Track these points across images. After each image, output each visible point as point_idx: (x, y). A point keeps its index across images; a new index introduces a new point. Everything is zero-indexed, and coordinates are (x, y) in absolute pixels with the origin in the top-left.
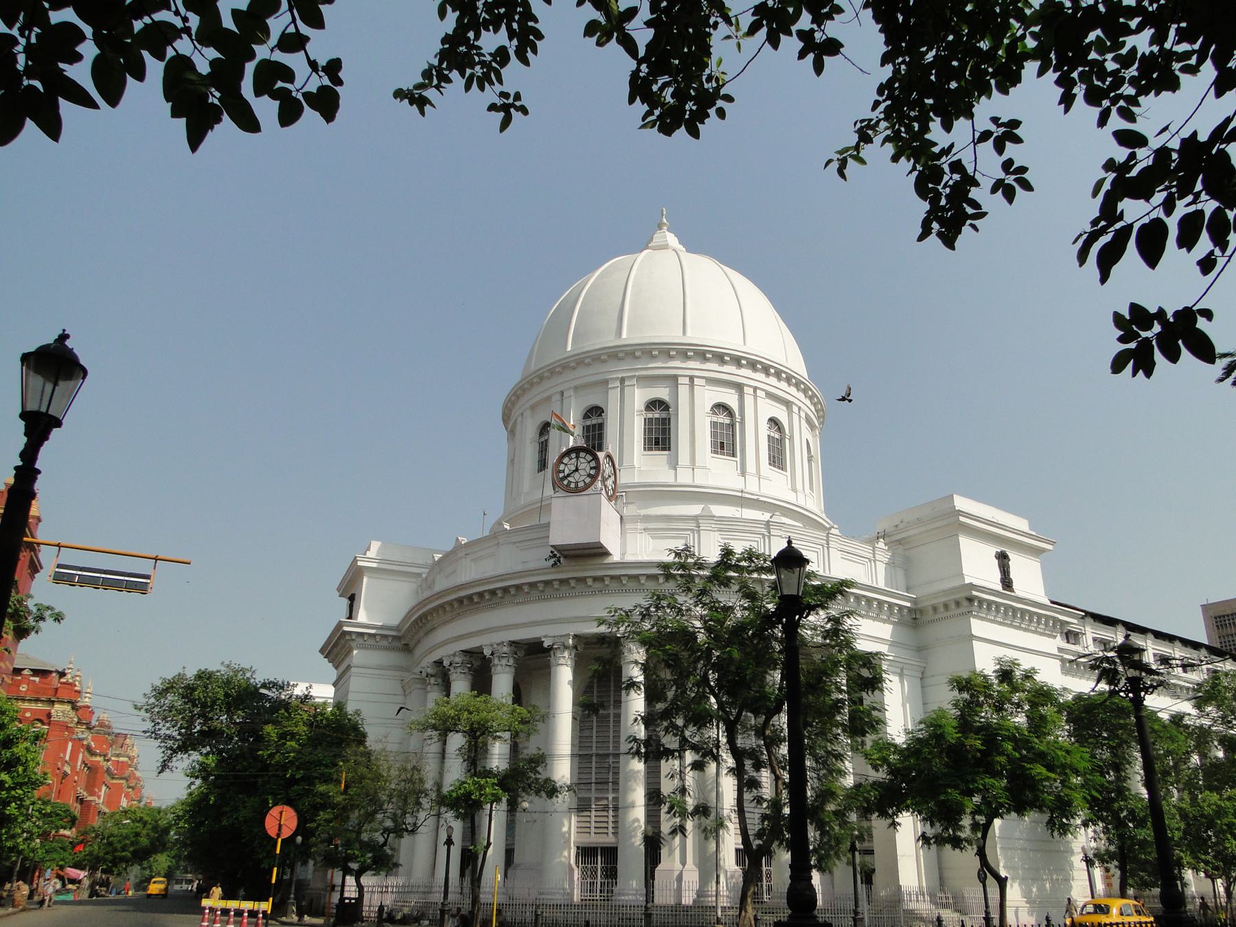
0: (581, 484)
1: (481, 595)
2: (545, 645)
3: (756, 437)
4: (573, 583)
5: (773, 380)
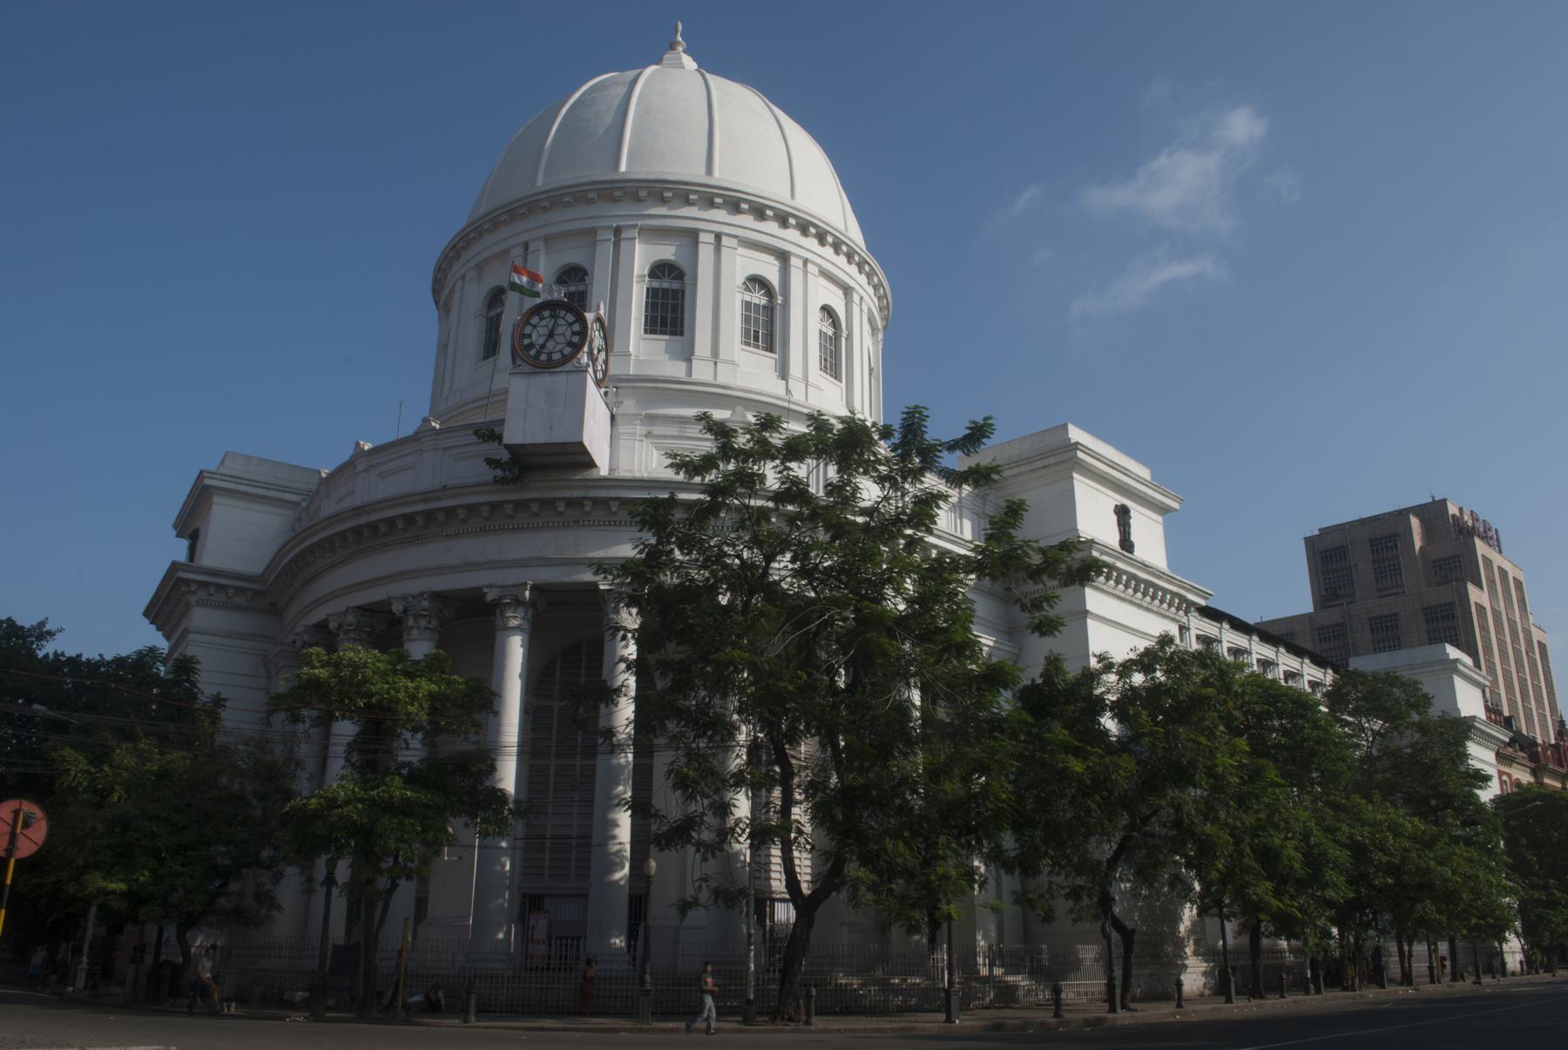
0: (557, 356)
1: (391, 522)
2: (489, 598)
3: (805, 330)
4: (535, 507)
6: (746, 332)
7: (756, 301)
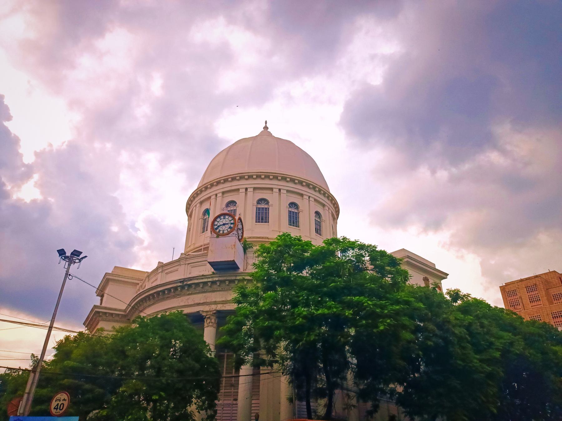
0: (225, 232)
5: (317, 194)
6: (290, 221)
7: (293, 210)
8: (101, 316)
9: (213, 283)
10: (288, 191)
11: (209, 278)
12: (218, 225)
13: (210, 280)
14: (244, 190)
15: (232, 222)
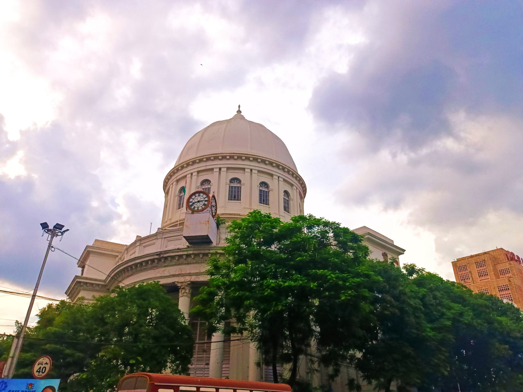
0: (200, 208)
7: (264, 189)
8: (82, 286)
9: (188, 256)
10: (259, 171)
11: (184, 251)
12: (193, 202)
13: (185, 253)
14: (218, 170)
15: (206, 199)
